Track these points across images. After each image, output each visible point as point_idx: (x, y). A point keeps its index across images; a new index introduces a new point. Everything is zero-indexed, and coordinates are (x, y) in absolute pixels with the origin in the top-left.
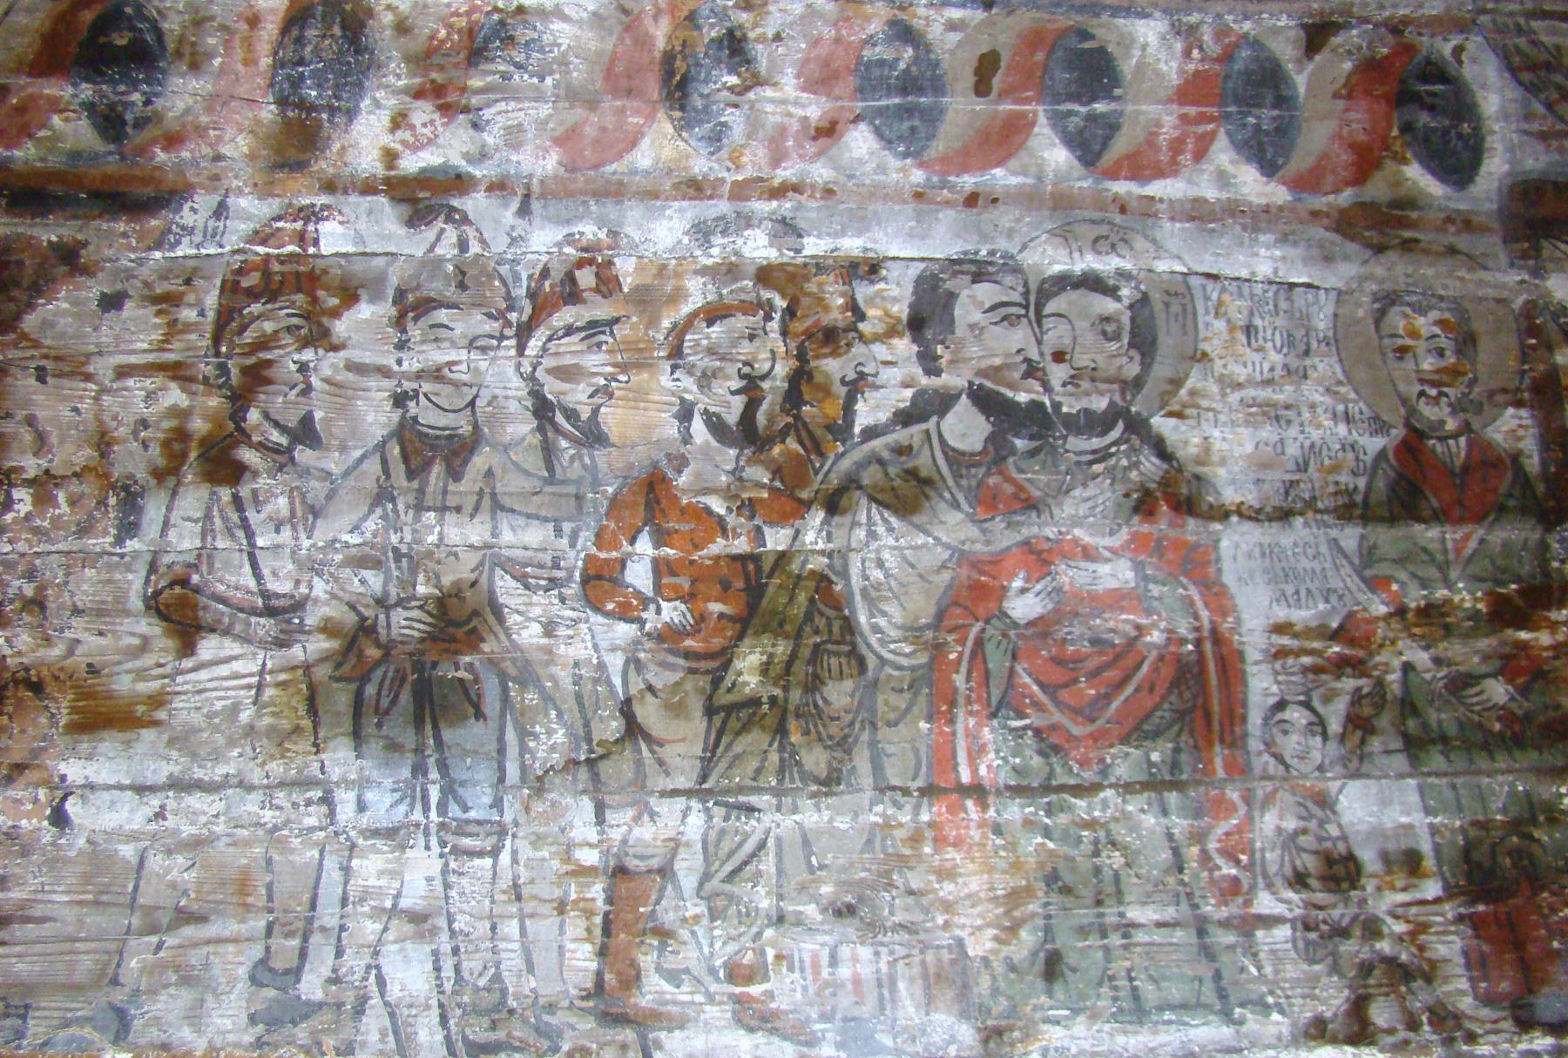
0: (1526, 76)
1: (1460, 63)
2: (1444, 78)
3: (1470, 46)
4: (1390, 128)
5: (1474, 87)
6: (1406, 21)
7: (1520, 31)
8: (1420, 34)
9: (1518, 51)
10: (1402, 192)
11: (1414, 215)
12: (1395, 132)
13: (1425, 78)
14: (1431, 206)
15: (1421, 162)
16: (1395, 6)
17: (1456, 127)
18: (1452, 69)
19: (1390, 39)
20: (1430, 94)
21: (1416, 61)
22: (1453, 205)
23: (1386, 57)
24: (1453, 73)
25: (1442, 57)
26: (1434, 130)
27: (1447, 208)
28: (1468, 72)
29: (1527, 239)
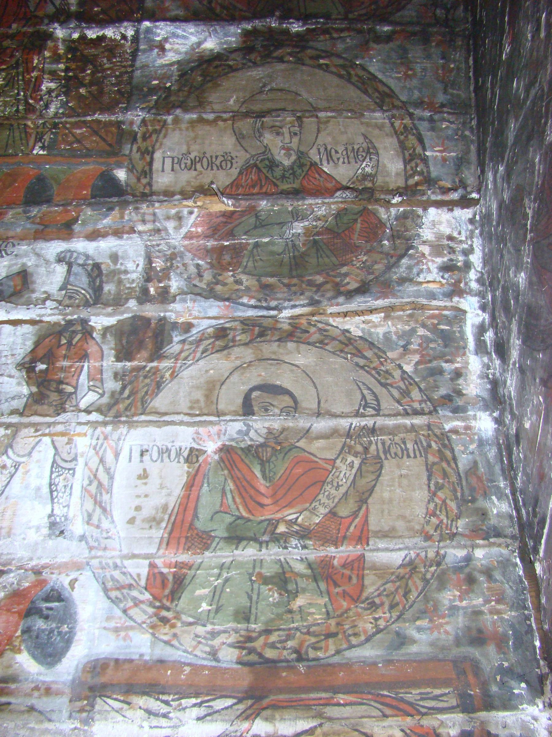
0: (114, 594)
1: (73, 588)
2: (59, 598)
3: (82, 578)
4: (16, 631)
5: (77, 603)
6: (44, 567)
7: (116, 566)
8: (52, 573)
9: (113, 578)
10: (10, 672)
11: (13, 686)
12: (19, 633)
13: (47, 599)
14: (26, 680)
15: (29, 651)
16: (39, 558)
17: (58, 628)
18: (66, 594)
19: (32, 577)
20: (48, 608)
21: (45, 589)
22: (41, 678)
23: (29, 587)
24: (67, 595)
25: (63, 586)
26: (43, 631)
27: (37, 680)
28: (77, 595)
29: (87, 698)
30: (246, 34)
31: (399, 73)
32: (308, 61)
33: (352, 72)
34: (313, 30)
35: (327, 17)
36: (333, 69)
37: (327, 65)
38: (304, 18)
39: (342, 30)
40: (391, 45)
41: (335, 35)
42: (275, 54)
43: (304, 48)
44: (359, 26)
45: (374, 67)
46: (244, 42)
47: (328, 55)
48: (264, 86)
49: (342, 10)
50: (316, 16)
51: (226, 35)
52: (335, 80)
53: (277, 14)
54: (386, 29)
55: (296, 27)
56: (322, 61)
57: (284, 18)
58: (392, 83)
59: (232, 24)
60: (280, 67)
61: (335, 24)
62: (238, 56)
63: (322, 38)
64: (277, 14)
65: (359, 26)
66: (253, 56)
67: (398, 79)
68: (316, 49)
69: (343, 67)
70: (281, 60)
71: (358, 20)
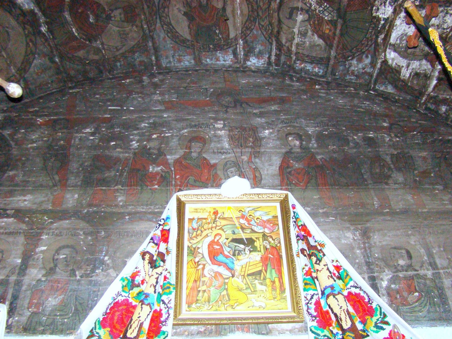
30: (32, 12)
31: (38, 70)
32: (28, 39)
33: (29, 56)
34: (45, 36)
35: (54, 38)
36: (29, 49)
37: (29, 47)
38: (50, 30)
39: (49, 45)
40: (50, 64)
41: (46, 44)
42: (26, 26)
43: (34, 35)
44: (54, 51)
45: (37, 62)
46: (27, 12)
47: (35, 45)
48: (7, 28)
49: (60, 42)
50: (53, 34)
51: (28, 4)
52: (23, 51)
53: (48, 20)
54: (57, 60)
55: (44, 29)
56: (31, 44)
57: (47, 23)
58: (32, 70)
59: (34, 4)
60: (21, 30)
61: (52, 42)
62: (18, 12)
63: (43, 40)
64: (48, 20)
65: (54, 51)
66: (22, 18)
67: (34, 71)
68: (36, 40)
69: (31, 52)
70: (24, 29)
71: (57, 49)
